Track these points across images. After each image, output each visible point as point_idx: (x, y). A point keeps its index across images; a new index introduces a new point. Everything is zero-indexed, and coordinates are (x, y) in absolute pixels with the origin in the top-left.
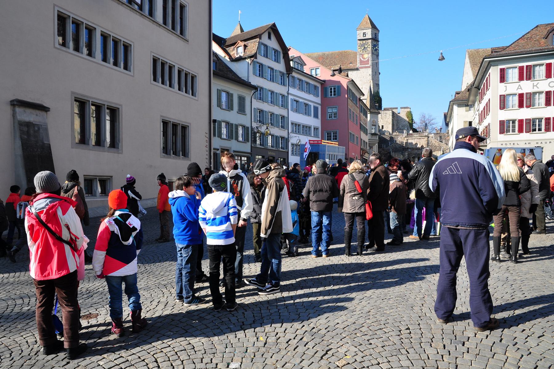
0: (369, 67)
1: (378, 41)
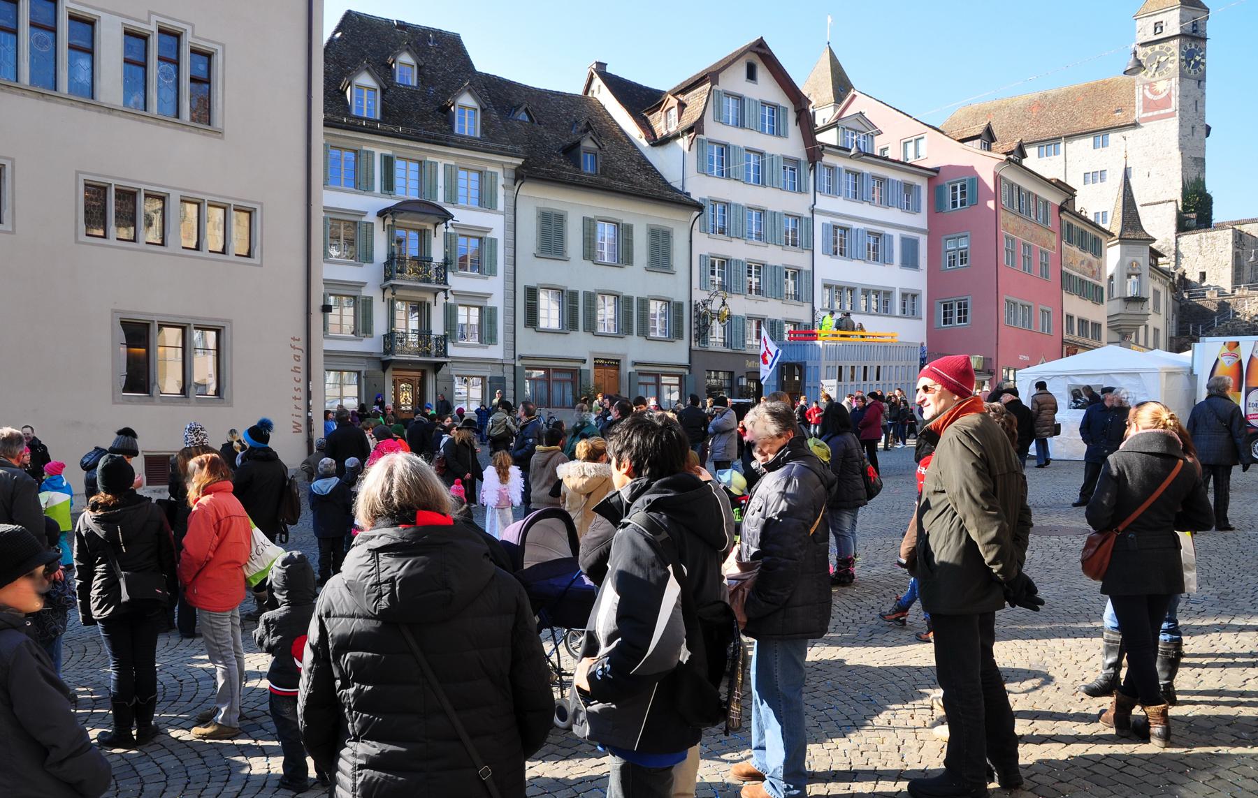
0: (1171, 115)
1: (1205, 39)
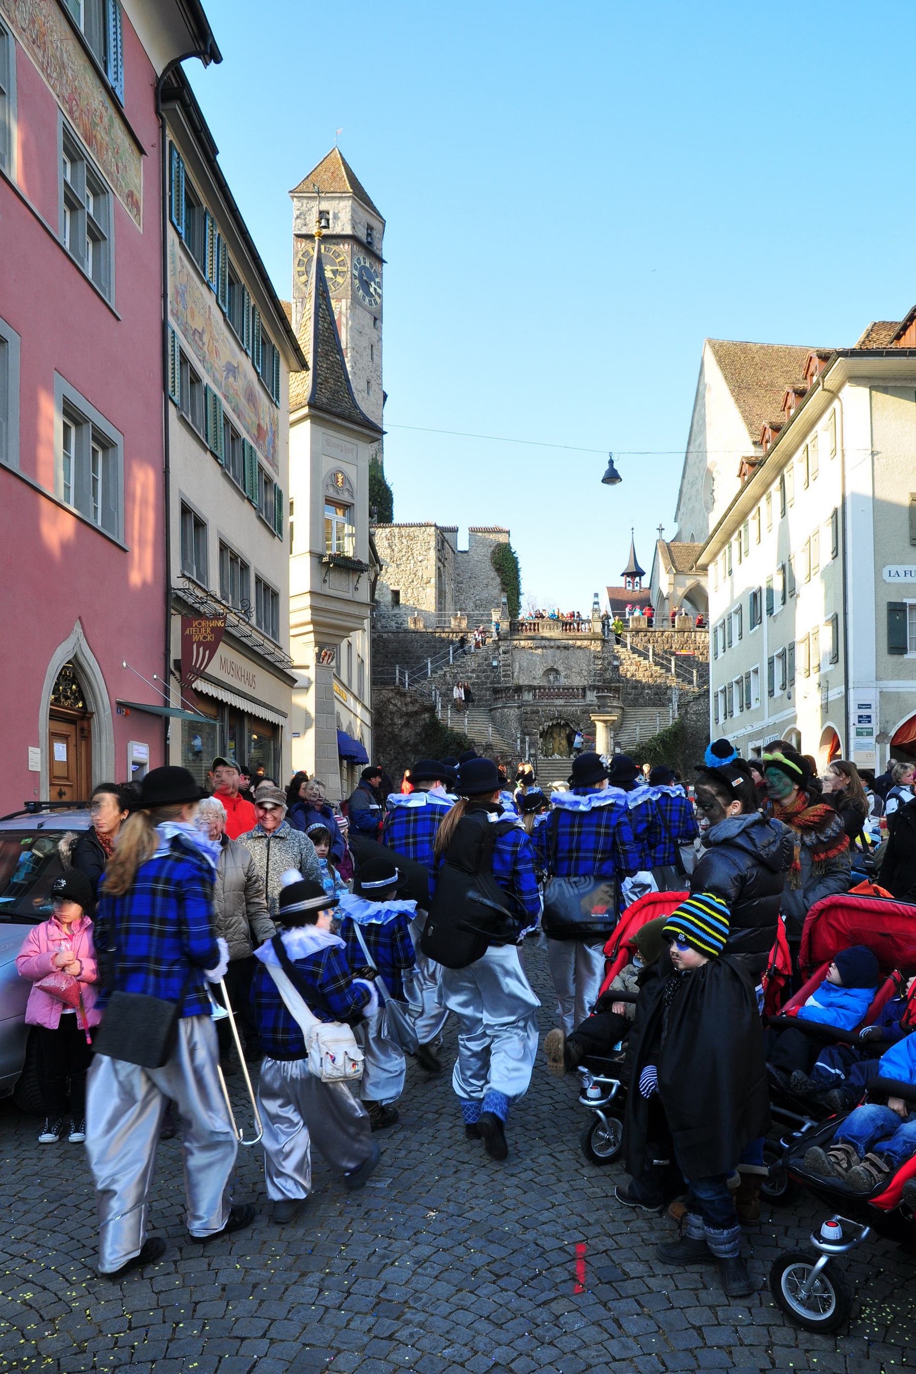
1: (381, 261)
